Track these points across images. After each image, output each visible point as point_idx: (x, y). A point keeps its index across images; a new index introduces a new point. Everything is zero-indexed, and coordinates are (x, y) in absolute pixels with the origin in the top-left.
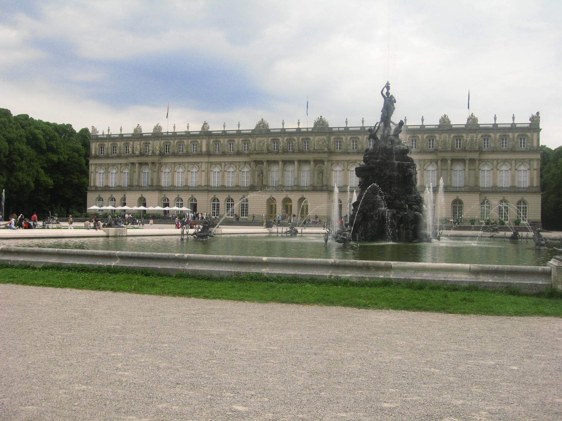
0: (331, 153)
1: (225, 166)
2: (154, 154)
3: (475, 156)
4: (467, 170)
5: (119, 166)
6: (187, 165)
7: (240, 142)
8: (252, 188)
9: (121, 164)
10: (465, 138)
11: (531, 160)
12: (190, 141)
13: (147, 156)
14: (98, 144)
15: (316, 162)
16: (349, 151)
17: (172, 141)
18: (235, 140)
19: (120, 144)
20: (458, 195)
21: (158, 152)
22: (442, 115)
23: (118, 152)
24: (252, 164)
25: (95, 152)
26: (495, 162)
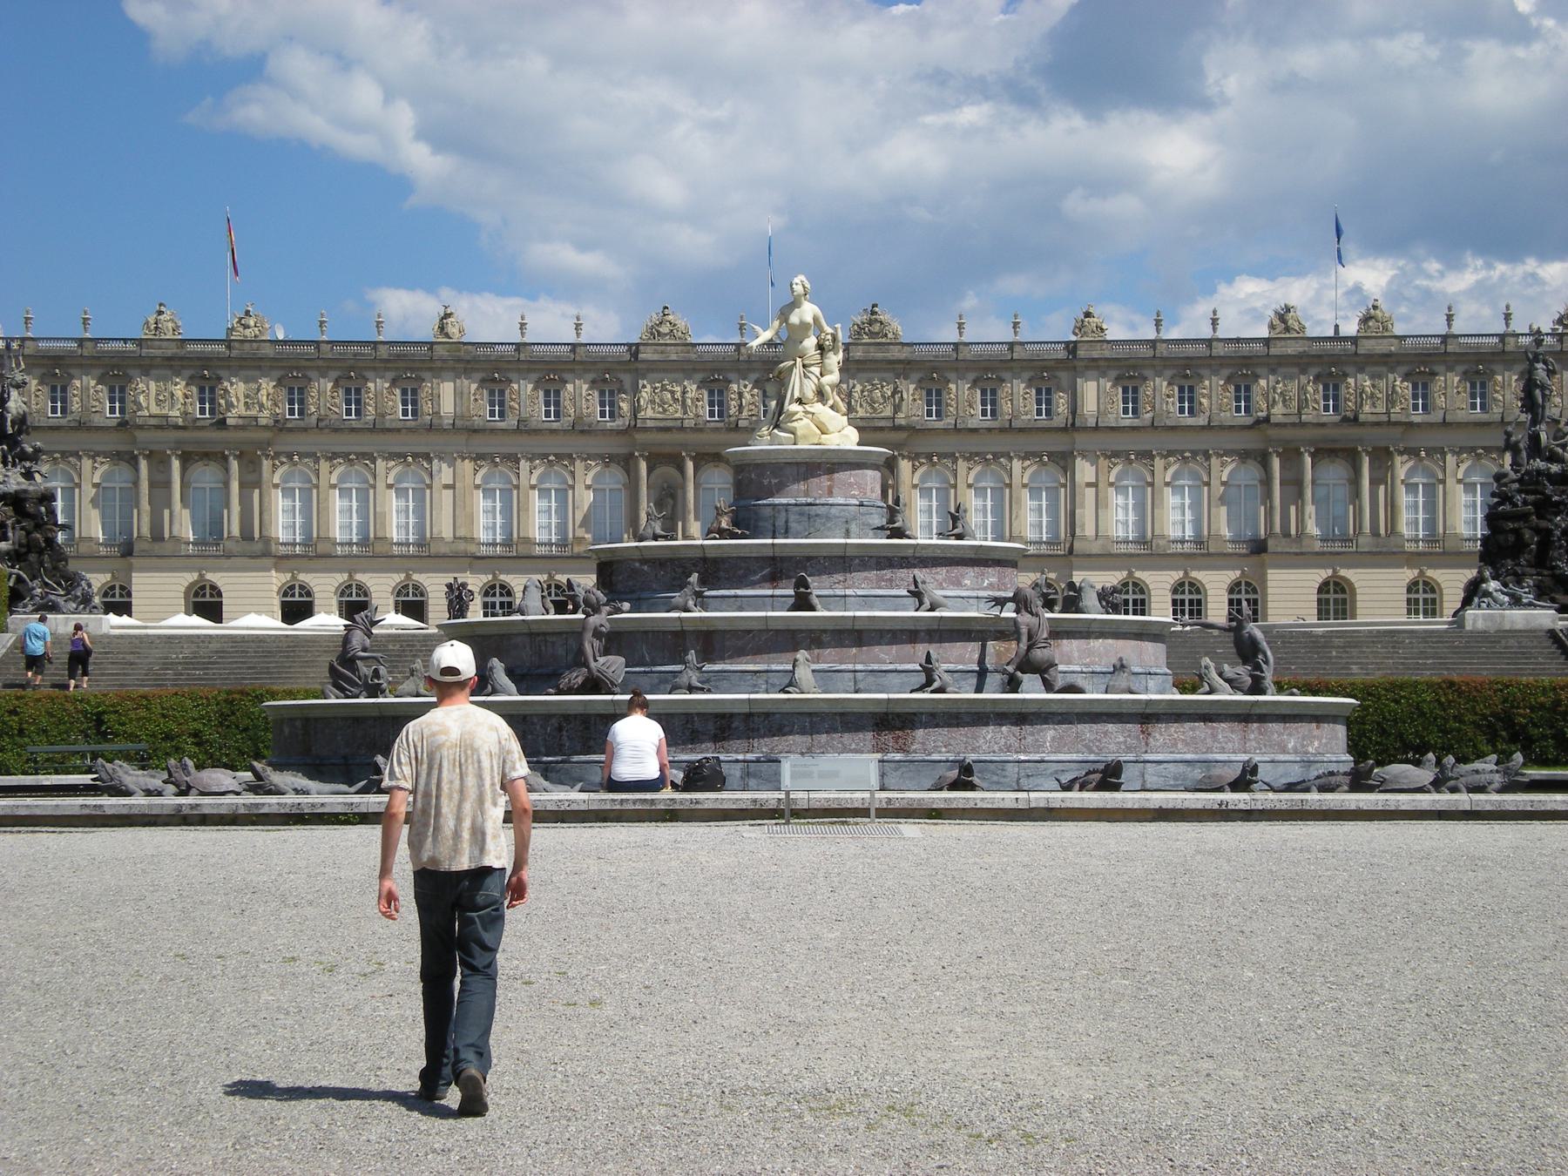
16: (973, 423)
21: (266, 413)
22: (1279, 306)
23: (75, 406)
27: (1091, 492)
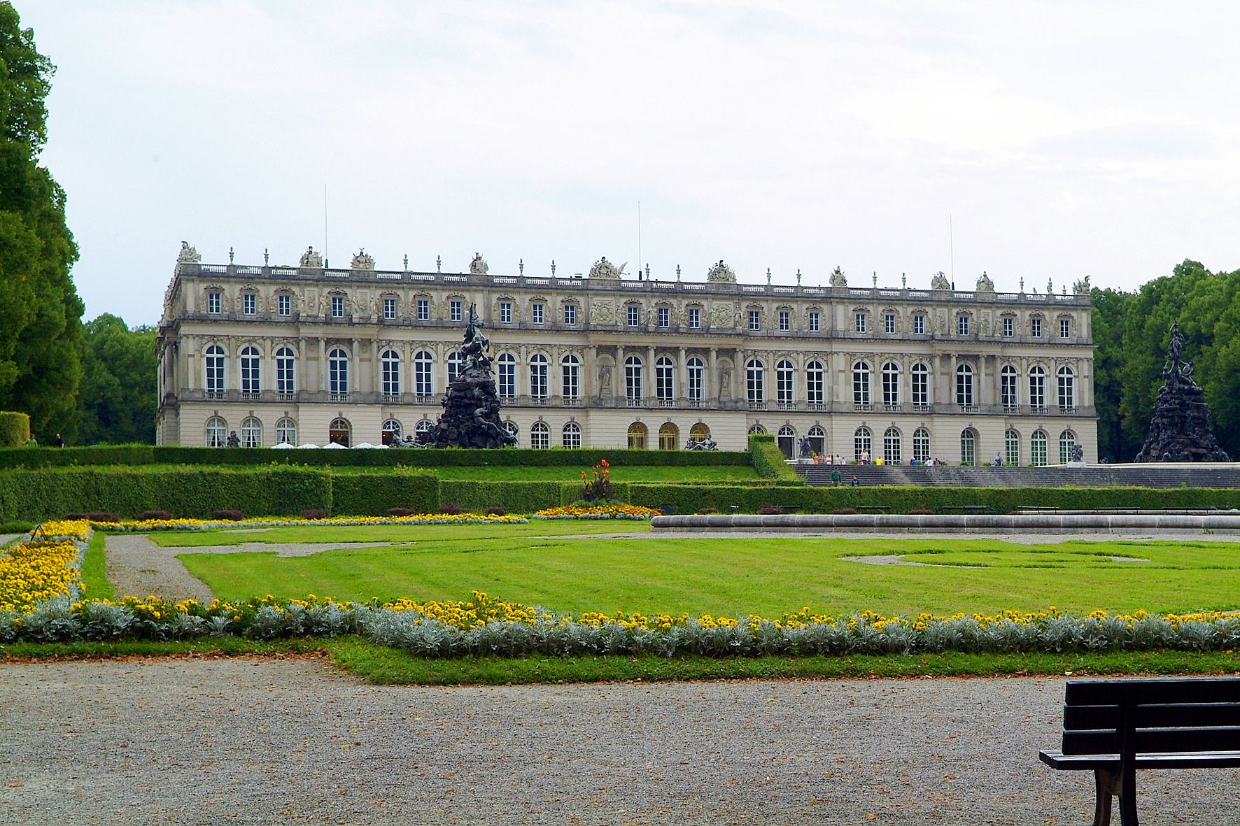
0: (745, 336)
1: (528, 353)
2: (365, 322)
3: (996, 351)
4: (983, 375)
5: (268, 343)
6: (440, 347)
7: (559, 304)
8: (597, 404)
9: (272, 339)
10: (974, 316)
11: (1078, 360)
12: (445, 294)
13: (351, 323)
14: (203, 286)
15: (720, 352)
17: (400, 293)
18: (547, 297)
19: (267, 292)
20: (971, 420)
22: (935, 272)
24: (594, 352)
25: (197, 306)
26: (1024, 362)
27: (842, 375)
